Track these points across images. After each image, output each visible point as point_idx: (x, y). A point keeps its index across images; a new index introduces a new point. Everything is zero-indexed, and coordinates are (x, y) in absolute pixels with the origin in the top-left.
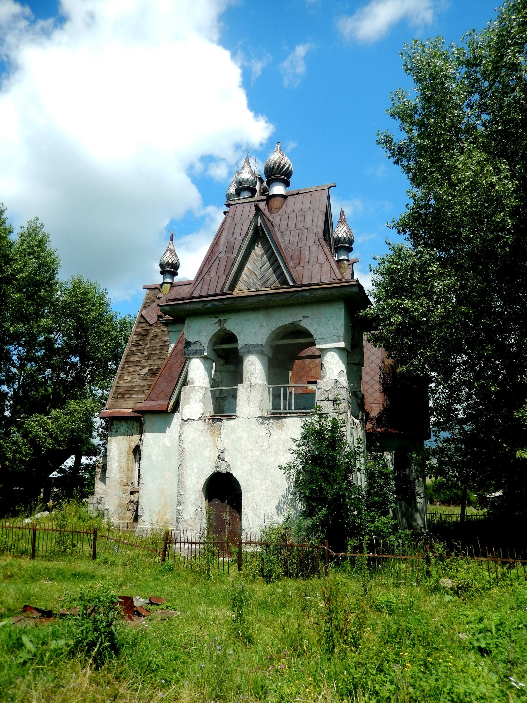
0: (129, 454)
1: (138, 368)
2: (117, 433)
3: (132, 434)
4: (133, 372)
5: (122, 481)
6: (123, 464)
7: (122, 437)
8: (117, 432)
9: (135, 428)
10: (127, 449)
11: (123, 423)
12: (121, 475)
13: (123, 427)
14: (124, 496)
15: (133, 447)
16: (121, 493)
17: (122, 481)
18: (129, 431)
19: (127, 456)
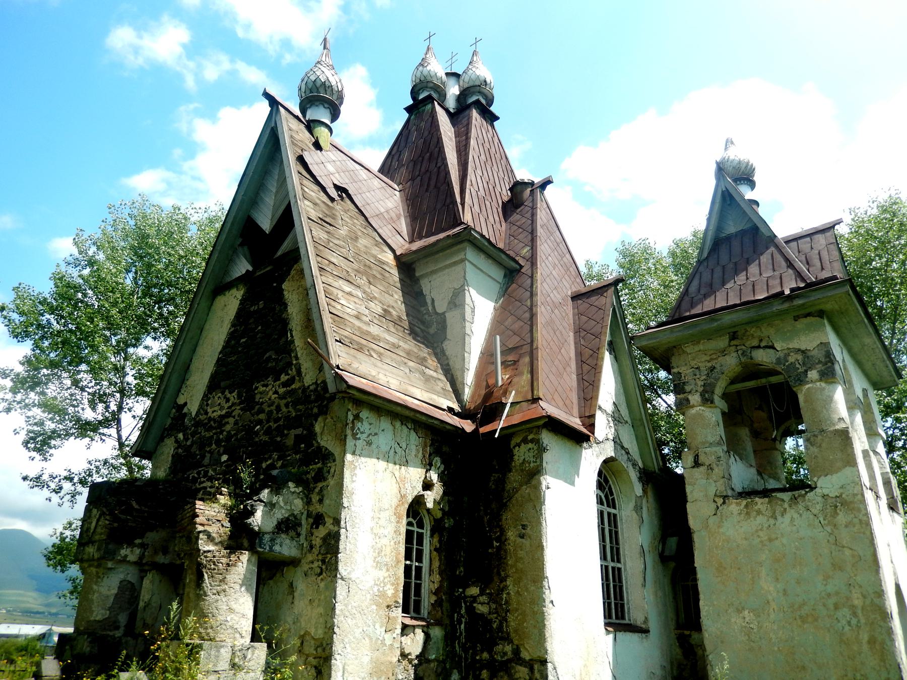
0: (399, 517)
1: (359, 293)
2: (370, 450)
3: (406, 463)
4: (350, 294)
5: (383, 595)
6: (385, 541)
7: (382, 464)
8: (369, 444)
9: (413, 447)
10: (395, 502)
11: (385, 423)
12: (383, 574)
13: (387, 434)
14: (388, 638)
15: (410, 499)
16: (380, 630)
17: (383, 595)
18: (398, 450)
19: (393, 519)
